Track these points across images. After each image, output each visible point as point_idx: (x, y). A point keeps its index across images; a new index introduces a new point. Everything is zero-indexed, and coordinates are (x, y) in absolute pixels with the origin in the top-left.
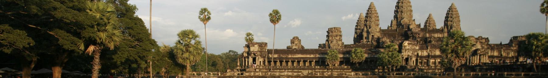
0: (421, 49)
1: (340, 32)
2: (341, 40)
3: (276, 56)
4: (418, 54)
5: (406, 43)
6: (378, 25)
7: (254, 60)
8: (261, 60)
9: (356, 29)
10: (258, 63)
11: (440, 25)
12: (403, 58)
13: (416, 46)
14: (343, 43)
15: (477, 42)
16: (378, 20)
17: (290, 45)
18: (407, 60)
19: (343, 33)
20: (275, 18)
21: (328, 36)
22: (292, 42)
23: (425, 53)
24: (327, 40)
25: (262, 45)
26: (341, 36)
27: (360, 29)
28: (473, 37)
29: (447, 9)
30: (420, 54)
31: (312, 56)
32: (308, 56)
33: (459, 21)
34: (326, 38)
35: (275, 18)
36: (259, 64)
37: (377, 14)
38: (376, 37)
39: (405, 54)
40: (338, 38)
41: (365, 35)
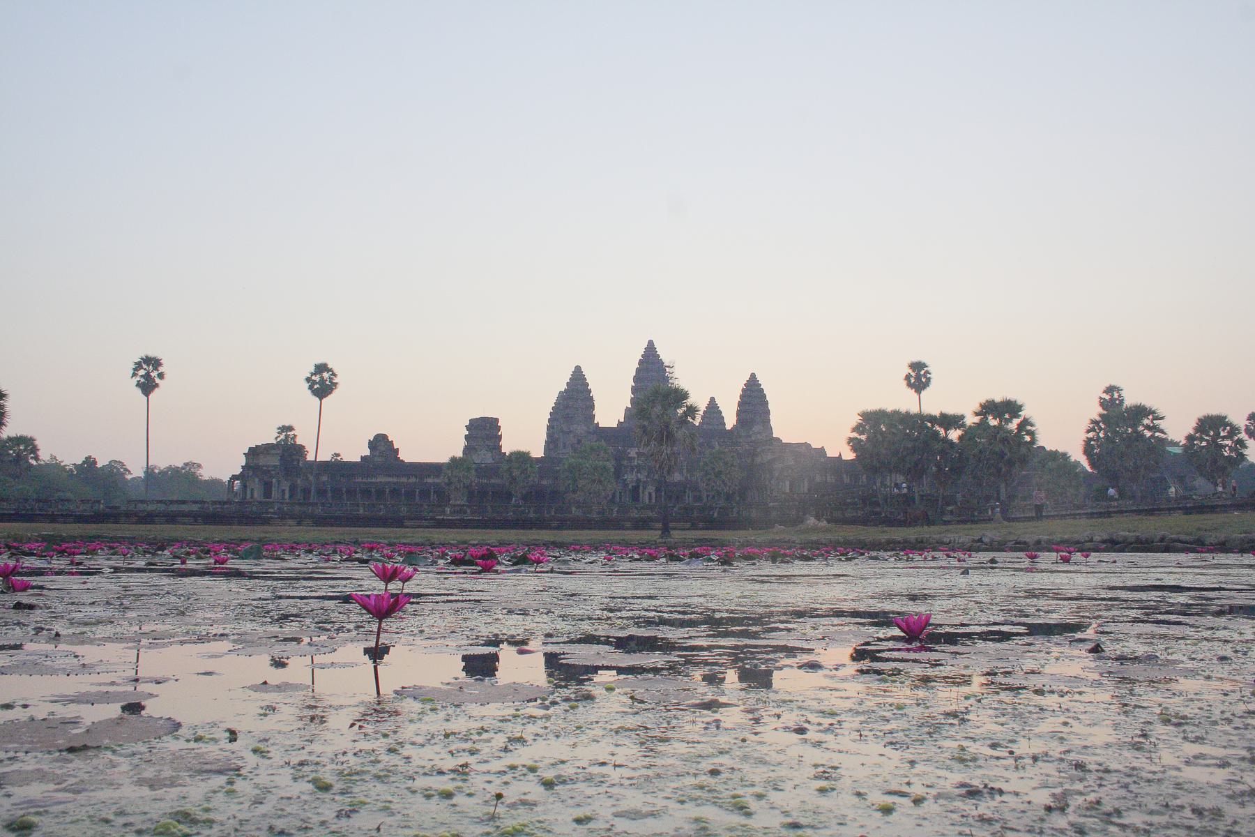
3: (324, 478)
11: (730, 421)
16: (592, 407)
17: (367, 452)
19: (503, 431)
22: (373, 445)
23: (677, 477)
31: (413, 480)
32: (404, 480)
33: (768, 412)
39: (630, 477)
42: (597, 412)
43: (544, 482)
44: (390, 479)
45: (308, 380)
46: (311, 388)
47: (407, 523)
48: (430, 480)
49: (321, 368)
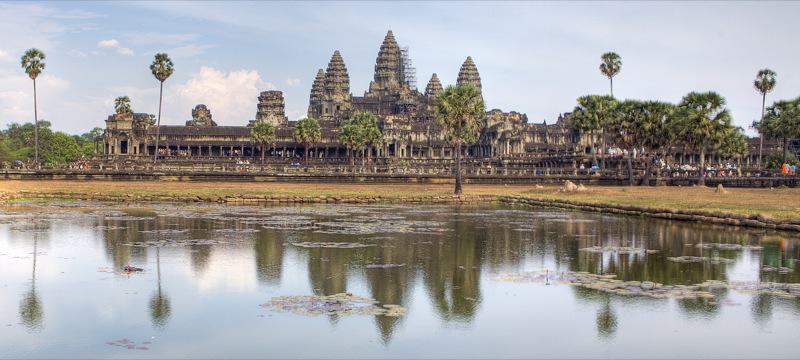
0: (416, 130)
1: (282, 99)
2: (283, 114)
3: (164, 139)
4: (410, 138)
5: (390, 119)
6: (347, 90)
7: (124, 146)
8: (136, 144)
9: (312, 96)
10: (130, 150)
12: (385, 144)
13: (408, 124)
14: (286, 118)
15: (505, 120)
16: (347, 82)
17: (191, 119)
18: (392, 148)
19: (286, 102)
20: (161, 69)
21: (260, 106)
22: (195, 114)
23: (422, 137)
24: (260, 115)
25: (139, 119)
26: (282, 106)
27: (315, 96)
28: (499, 110)
29: (460, 66)
30: (413, 139)
31: (228, 139)
32: (222, 139)
34: (256, 110)
35: (161, 69)
36: (133, 152)
37: (346, 70)
38: (342, 108)
39: (388, 138)
40: (277, 110)
41: (325, 105)
42: (352, 85)
43: (324, 141)
44: (212, 139)
45: (152, 67)
46: (154, 73)
47: (256, 178)
48: (241, 140)
49: (160, 58)
